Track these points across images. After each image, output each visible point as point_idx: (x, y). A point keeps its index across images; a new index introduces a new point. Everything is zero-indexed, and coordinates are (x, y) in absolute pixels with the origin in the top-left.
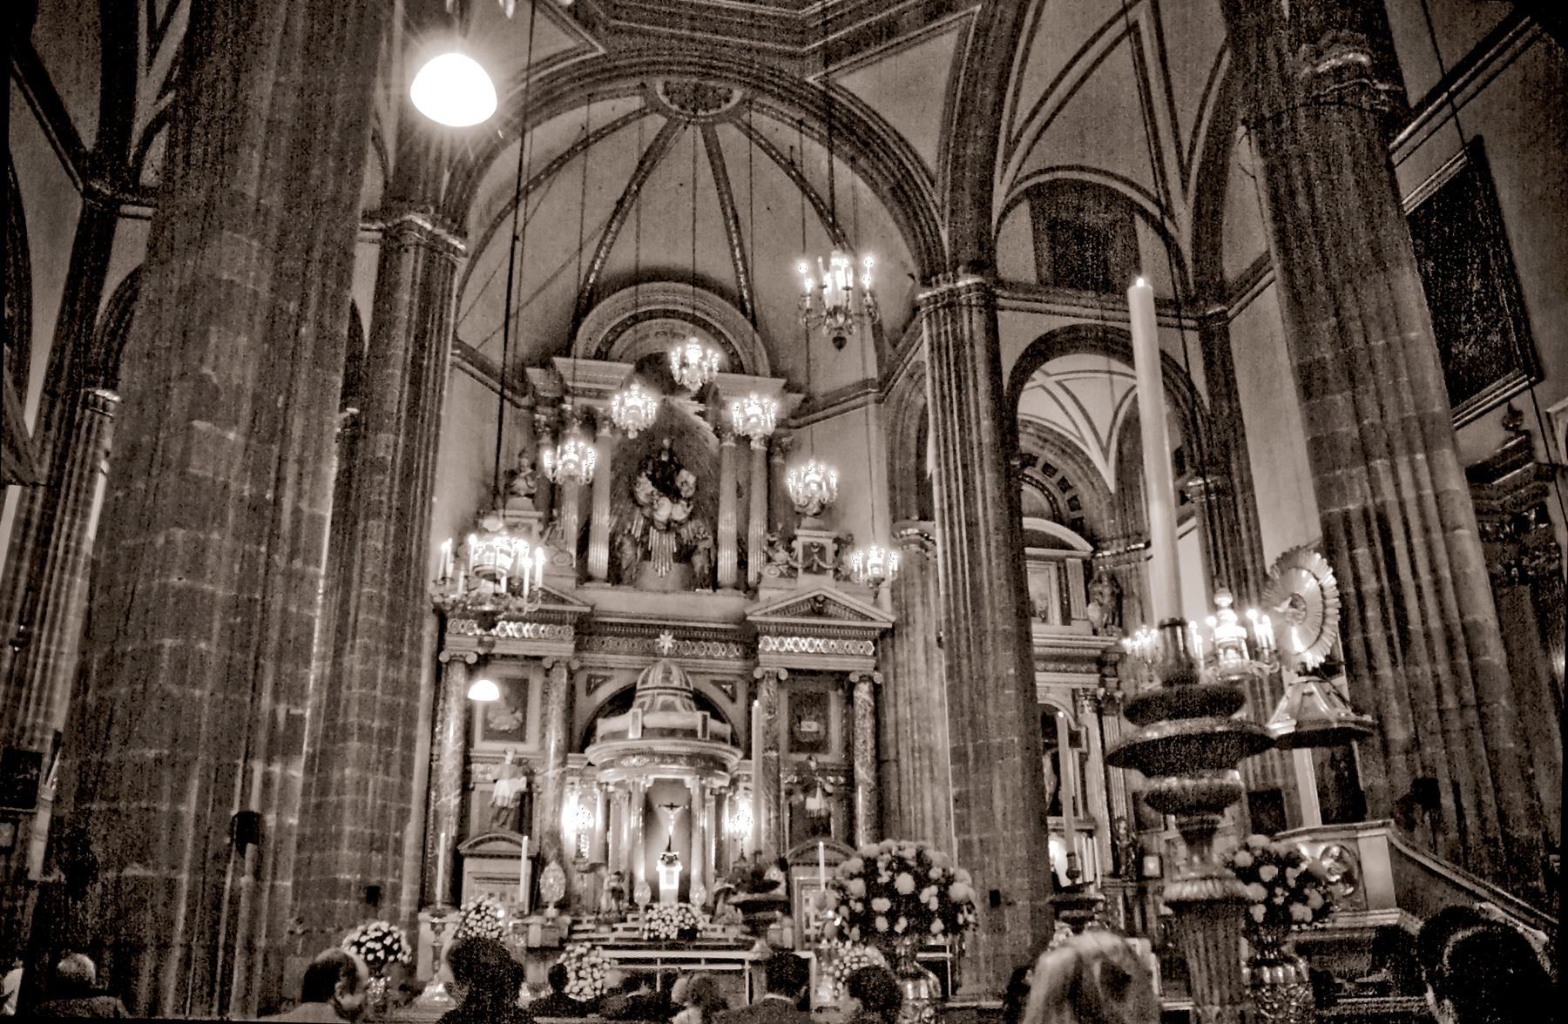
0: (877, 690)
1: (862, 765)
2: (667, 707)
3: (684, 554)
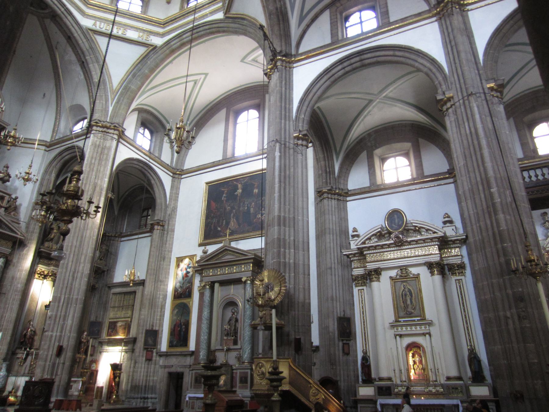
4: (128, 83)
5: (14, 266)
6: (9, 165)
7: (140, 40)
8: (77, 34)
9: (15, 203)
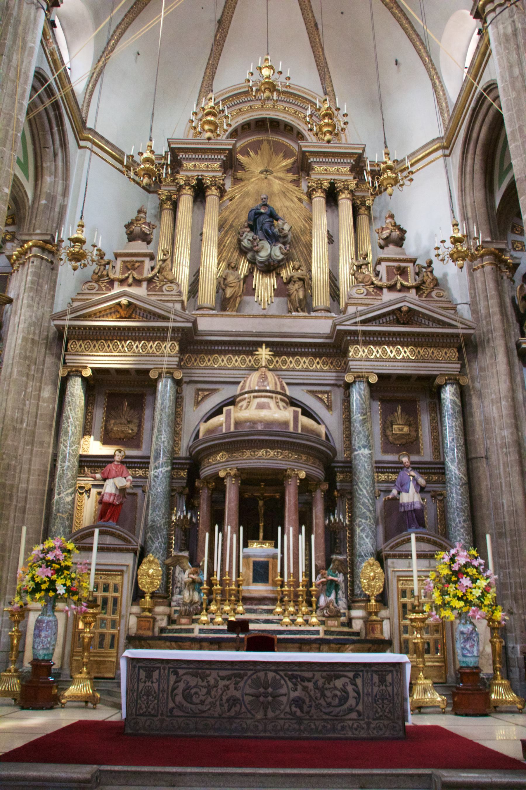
0: (463, 394)
1: (453, 461)
2: (261, 407)
5: (480, 396)
6: (393, 213)
9: (431, 272)
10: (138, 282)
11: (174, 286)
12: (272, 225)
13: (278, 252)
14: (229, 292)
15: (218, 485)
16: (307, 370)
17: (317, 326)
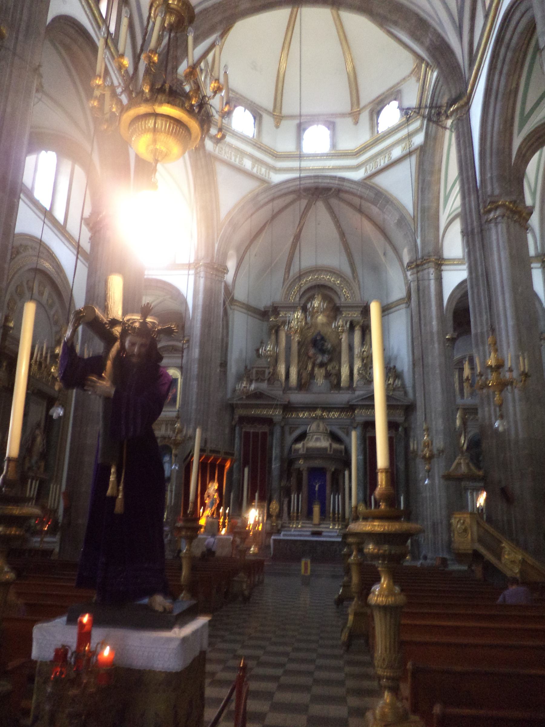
2: (317, 440)
3: (328, 376)
4: (422, 204)
7: (405, 152)
8: (360, 190)
9: (395, 371)
10: (263, 381)
11: (279, 383)
12: (323, 345)
13: (326, 358)
14: (303, 381)
15: (299, 473)
16: (337, 418)
17: (342, 398)
